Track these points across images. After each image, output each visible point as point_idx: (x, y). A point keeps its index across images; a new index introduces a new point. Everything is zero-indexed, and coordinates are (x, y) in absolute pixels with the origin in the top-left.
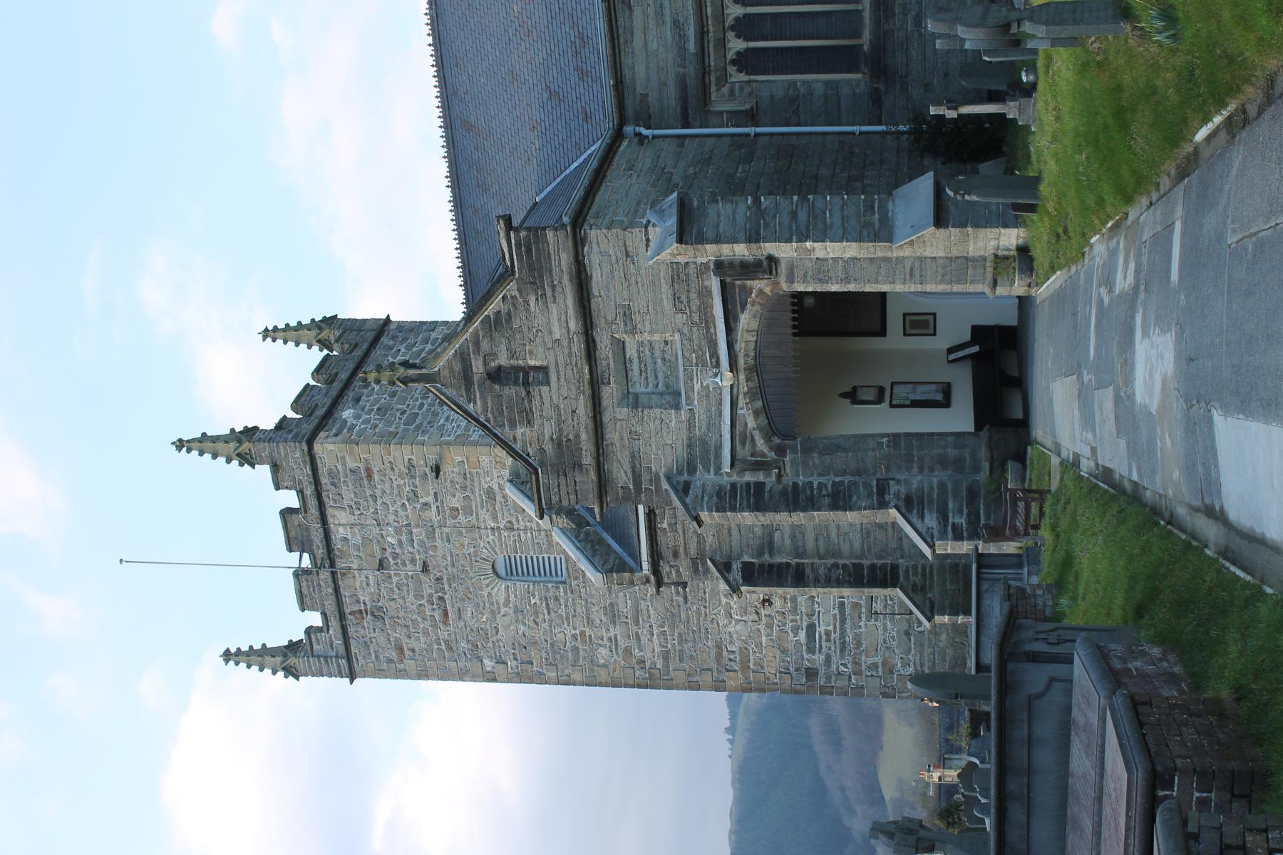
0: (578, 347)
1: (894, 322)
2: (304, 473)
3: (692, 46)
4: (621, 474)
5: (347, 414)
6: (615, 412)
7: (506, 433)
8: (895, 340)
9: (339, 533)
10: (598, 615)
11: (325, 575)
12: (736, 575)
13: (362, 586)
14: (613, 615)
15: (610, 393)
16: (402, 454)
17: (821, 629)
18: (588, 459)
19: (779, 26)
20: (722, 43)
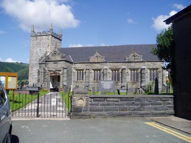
0: (57, 60)
1: (59, 83)
2: (49, 34)
3: (79, 68)
4: (47, 63)
5: (54, 38)
6: (52, 62)
7: (51, 54)
8: (57, 83)
9: (44, 36)
10: (36, 58)
11: (40, 35)
12: (39, 70)
13: (39, 37)
14: (36, 59)
15: (54, 62)
16: (50, 42)
17: (34, 76)
18: (49, 60)
19: (80, 75)
20: (79, 71)
